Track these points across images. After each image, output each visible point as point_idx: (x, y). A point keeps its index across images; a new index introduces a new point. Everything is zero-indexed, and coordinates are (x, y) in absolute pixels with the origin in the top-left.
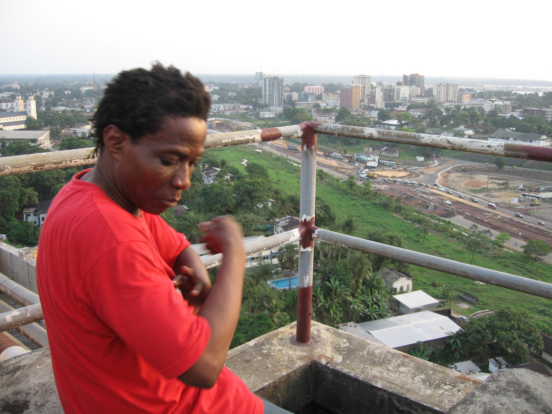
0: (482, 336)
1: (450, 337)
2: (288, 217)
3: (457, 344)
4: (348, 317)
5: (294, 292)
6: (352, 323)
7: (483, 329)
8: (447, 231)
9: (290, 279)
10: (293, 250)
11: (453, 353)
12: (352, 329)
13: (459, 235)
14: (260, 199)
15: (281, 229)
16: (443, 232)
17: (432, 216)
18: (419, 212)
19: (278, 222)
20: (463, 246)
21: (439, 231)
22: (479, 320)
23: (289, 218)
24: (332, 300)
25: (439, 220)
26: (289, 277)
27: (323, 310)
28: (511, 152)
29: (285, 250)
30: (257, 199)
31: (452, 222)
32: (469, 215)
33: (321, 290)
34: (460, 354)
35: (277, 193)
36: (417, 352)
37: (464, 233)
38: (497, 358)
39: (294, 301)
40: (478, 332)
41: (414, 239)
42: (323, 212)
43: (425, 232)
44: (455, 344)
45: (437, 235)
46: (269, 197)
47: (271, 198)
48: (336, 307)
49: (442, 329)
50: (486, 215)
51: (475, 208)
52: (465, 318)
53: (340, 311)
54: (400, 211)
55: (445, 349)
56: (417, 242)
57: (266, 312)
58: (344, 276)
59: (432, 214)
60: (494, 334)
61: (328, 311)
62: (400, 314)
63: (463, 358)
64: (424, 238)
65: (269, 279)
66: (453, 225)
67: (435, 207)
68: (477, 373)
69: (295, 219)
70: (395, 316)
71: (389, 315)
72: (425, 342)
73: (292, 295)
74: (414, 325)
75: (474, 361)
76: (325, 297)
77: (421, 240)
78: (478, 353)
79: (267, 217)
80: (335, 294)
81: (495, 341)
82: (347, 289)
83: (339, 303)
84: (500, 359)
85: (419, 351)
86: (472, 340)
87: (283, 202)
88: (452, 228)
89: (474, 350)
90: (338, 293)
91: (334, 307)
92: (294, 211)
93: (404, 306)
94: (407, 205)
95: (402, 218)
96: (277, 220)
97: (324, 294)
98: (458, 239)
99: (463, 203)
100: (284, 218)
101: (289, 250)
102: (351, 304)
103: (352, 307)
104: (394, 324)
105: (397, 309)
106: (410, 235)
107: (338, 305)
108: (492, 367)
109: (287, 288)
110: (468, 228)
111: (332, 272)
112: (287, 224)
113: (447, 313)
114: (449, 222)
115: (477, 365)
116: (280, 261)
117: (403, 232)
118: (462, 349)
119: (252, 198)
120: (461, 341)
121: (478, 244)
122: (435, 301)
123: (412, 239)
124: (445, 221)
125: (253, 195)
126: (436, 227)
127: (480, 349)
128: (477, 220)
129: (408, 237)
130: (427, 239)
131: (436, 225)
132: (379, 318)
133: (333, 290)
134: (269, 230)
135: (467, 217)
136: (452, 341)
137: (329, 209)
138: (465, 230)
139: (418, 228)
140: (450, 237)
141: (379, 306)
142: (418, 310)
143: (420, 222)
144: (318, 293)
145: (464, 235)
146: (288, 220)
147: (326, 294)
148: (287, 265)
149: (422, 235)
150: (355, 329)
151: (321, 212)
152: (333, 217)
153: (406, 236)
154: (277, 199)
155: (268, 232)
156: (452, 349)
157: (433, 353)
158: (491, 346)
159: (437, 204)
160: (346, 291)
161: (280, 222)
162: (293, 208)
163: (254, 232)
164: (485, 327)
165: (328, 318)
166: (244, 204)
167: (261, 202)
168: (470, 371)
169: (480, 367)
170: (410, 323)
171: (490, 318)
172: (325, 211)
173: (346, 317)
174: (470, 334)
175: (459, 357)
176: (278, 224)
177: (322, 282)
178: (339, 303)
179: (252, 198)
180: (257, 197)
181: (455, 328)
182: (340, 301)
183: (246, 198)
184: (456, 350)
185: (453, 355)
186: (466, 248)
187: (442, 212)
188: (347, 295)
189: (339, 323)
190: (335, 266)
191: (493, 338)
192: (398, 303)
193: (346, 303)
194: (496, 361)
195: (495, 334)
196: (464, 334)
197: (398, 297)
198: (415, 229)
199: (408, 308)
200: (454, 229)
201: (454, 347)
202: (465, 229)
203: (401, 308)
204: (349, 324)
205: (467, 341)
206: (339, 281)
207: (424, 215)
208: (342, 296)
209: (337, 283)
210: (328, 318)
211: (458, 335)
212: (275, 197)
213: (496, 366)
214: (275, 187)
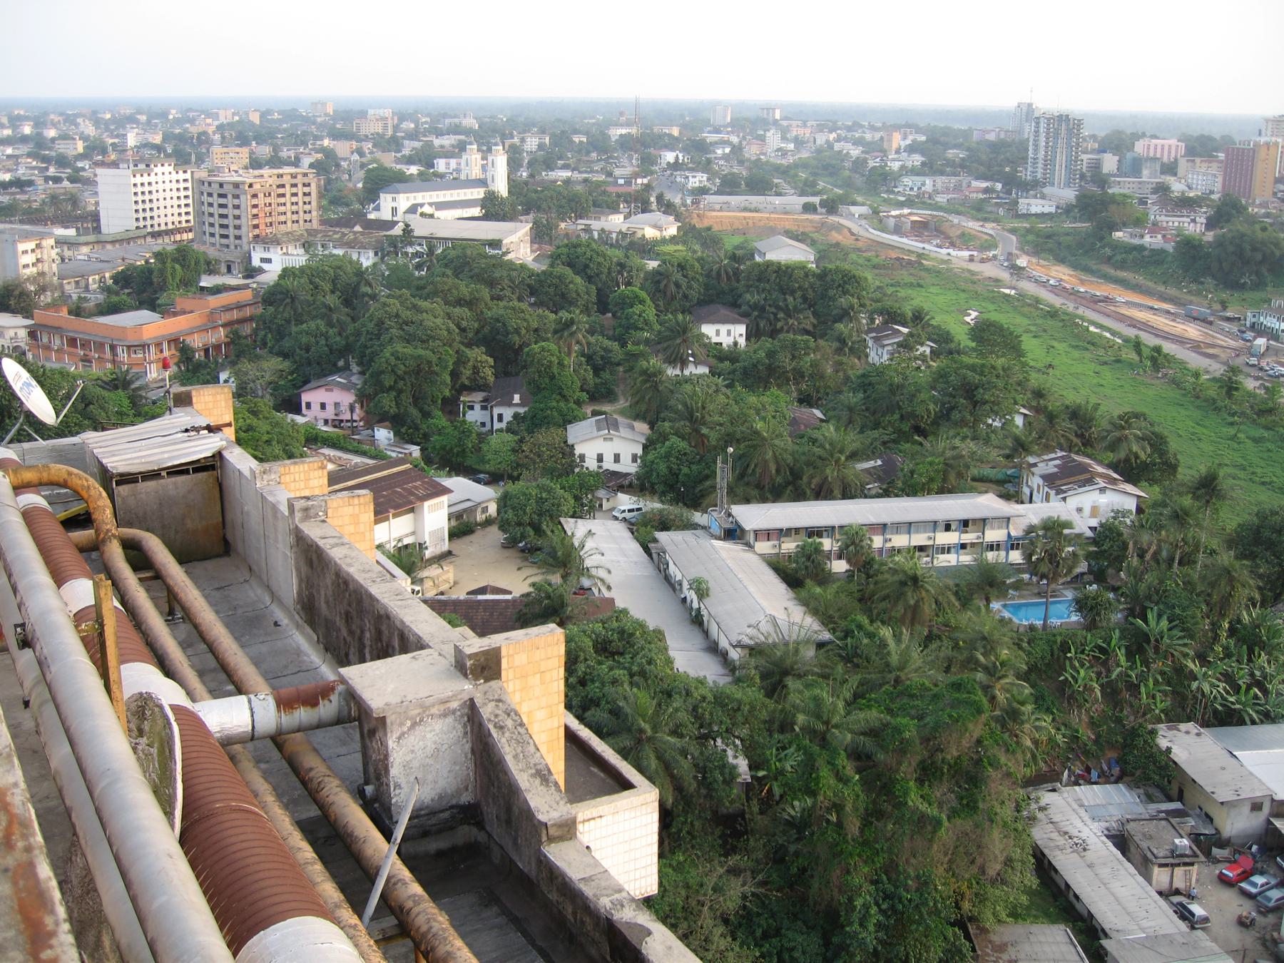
2: (1060, 454)
4: (1183, 709)
5: (1054, 635)
6: (1191, 726)
9: (1046, 603)
10: (1060, 534)
12: (1191, 739)
14: (996, 408)
15: (1041, 482)
19: (1035, 465)
24: (1146, 663)
29: (1040, 533)
30: (987, 407)
33: (1120, 639)
35: (1039, 394)
39: (1052, 655)
42: (1149, 450)
46: (1016, 403)
47: (1024, 407)
48: (1156, 682)
53: (1165, 693)
57: (980, 676)
58: (1184, 610)
61: (1134, 688)
65: (998, 598)
69: (1074, 461)
73: (1048, 641)
76: (1130, 655)
79: (1007, 451)
82: (1186, 641)
83: (1162, 673)
87: (1051, 417)
92: (1078, 441)
96: (1031, 460)
97: (1127, 647)
101: (1049, 534)
102: (1195, 679)
103: (1195, 685)
109: (1039, 623)
111: (1155, 598)
112: (1056, 470)
116: (1028, 557)
119: (975, 404)
125: (978, 397)
133: (1152, 639)
134: (1010, 482)
137: (1166, 442)
144: (1113, 642)
146: (1058, 462)
147: (1134, 648)
148: (1044, 568)
150: (1198, 739)
151: (1144, 449)
152: (1173, 461)
154: (1037, 410)
155: (1010, 488)
160: (1185, 645)
162: (1077, 435)
163: (975, 484)
165: (1132, 706)
166: (956, 415)
167: (996, 414)
173: (1179, 710)
176: (1033, 469)
177: (1127, 617)
178: (1162, 673)
179: (975, 404)
180: (985, 402)
183: (962, 401)
188: (1186, 655)
189: (1159, 721)
190: (1161, 582)
193: (1180, 676)
204: (1183, 726)
206: (1170, 621)
209: (1164, 624)
210: (1132, 706)
212: (1034, 403)
214: (1035, 380)
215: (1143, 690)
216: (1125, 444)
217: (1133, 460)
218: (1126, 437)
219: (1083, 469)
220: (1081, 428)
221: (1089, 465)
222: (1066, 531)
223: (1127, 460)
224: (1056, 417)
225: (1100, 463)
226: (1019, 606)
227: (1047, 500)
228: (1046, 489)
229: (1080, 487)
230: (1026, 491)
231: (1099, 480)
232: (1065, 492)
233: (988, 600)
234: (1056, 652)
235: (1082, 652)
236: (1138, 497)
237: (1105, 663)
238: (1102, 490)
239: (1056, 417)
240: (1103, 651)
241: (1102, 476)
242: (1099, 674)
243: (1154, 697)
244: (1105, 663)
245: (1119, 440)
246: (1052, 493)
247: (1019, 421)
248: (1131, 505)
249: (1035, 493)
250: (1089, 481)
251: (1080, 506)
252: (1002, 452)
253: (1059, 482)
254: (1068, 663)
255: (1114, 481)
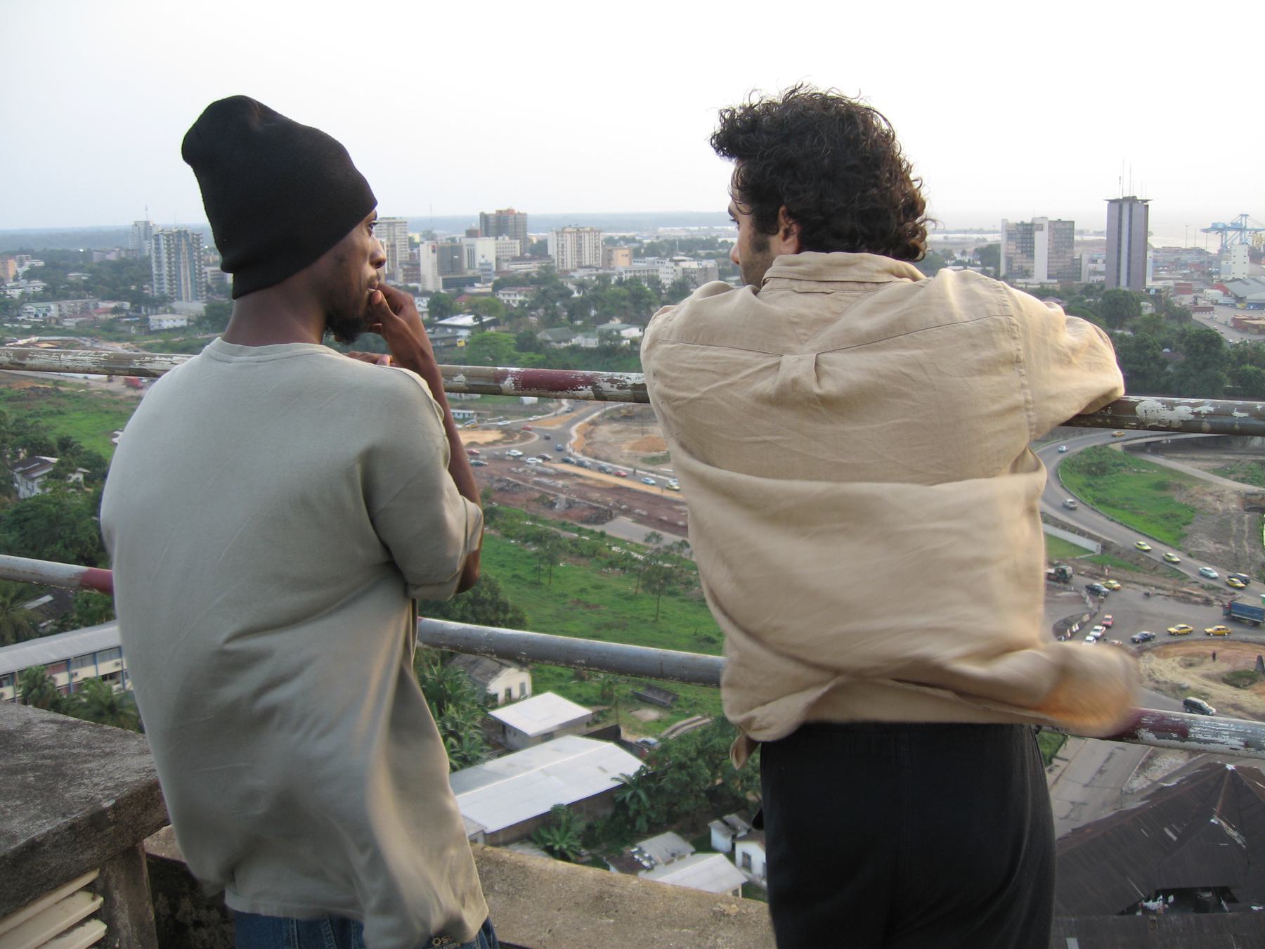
0: (689, 774)
1: (623, 787)
3: (640, 800)
7: (691, 760)
8: (599, 554)
11: (632, 822)
13: (626, 559)
16: (591, 556)
17: (564, 524)
18: (534, 519)
20: (635, 584)
21: (582, 555)
22: (680, 739)
25: (579, 530)
28: (530, 370)
31: (608, 532)
32: (645, 513)
34: (648, 820)
36: (555, 831)
37: (636, 555)
38: (727, 817)
40: (681, 766)
41: (529, 579)
43: (552, 561)
44: (635, 800)
45: (579, 565)
49: (604, 771)
50: (681, 511)
51: (656, 496)
52: (652, 740)
54: (492, 518)
55: (614, 816)
56: (536, 584)
59: (563, 520)
60: (715, 767)
62: (510, 750)
63: (655, 829)
64: (550, 574)
66: (611, 538)
67: (570, 505)
68: (688, 855)
70: (499, 756)
71: (484, 756)
72: (570, 805)
74: (542, 770)
75: (680, 832)
77: (545, 580)
78: (687, 813)
81: (719, 781)
84: (733, 818)
85: (558, 828)
86: (669, 786)
88: (610, 547)
89: (676, 808)
93: (516, 732)
94: (507, 505)
95: (498, 534)
98: (623, 569)
99: (629, 490)
104: (496, 775)
105: (500, 740)
106: (515, 572)
108: (719, 838)
110: (641, 542)
113: (612, 735)
114: (602, 535)
115: (686, 839)
117: (503, 566)
118: (652, 807)
120: (648, 791)
121: (668, 576)
122: (581, 711)
123: (524, 580)
124: (592, 532)
126: (574, 548)
127: (689, 804)
128: (663, 524)
129: (514, 576)
130: (558, 577)
131: (574, 543)
132: (462, 767)
135: (640, 520)
136: (629, 794)
138: (638, 548)
139: (537, 554)
140: (607, 567)
141: (459, 739)
142: (547, 736)
143: (539, 539)
145: (636, 560)
149: (545, 567)
153: (509, 574)
156: (631, 813)
157: (590, 828)
158: (713, 794)
159: (573, 497)
164: (693, 754)
168: (673, 855)
169: (694, 843)
170: (531, 768)
171: (704, 733)
174: (665, 773)
175: (645, 827)
181: (630, 765)
184: (638, 813)
185: (634, 826)
186: (643, 587)
187: (585, 513)
191: (714, 774)
192: (503, 727)
194: (726, 823)
195: (716, 767)
196: (652, 777)
197: (501, 714)
198: (529, 557)
199: (525, 735)
200: (614, 548)
201: (633, 807)
202: (638, 546)
203: (510, 738)
205: (660, 791)
207: (545, 522)
211: (640, 780)
213: (725, 835)
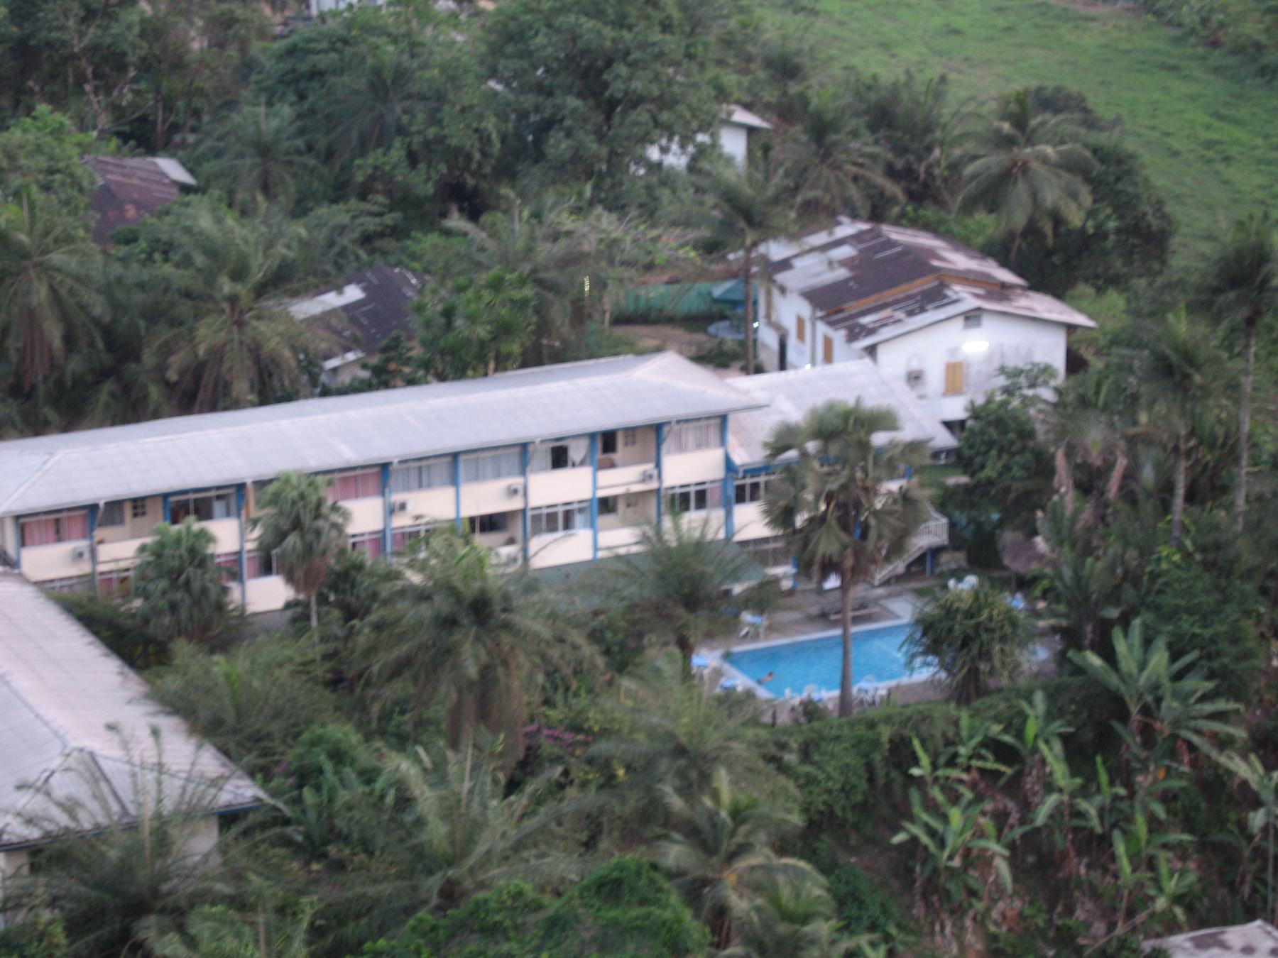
2: (847, 228)
5: (872, 725)
9: (845, 640)
10: (864, 446)
14: (665, 116)
15: (805, 309)
19: (785, 265)
23: (856, 238)
24: (1122, 774)
26: (842, 623)
27: (1061, 841)
29: (812, 446)
30: (641, 115)
33: (1050, 716)
39: (871, 780)
42: (1087, 199)
46: (722, 94)
47: (748, 107)
48: (1155, 825)
53: (1181, 852)
57: (676, 853)
69: (891, 244)
76: (1077, 755)
79: (704, 233)
80: (1147, 734)
83: (1167, 798)
87: (821, 129)
90: (1163, 727)
91: (1141, 826)
92: (894, 189)
96: (776, 250)
100: (820, 238)
101: (834, 449)
107: (1160, 811)
109: (828, 695)
112: (842, 273)
116: (782, 516)
119: (609, 107)
125: (617, 89)
133: (1134, 709)
134: (723, 317)
137: (1129, 172)
144: (1031, 729)
146: (846, 251)
147: (1088, 735)
148: (828, 544)
151: (1074, 196)
152: (1155, 223)
154: (786, 112)
155: (724, 333)
161: (798, 263)
162: (891, 172)
163: (621, 331)
166: (558, 145)
167: (670, 131)
172: (1096, 184)
176: (781, 277)
177: (1061, 658)
179: (609, 107)
180: (636, 102)
182: (1176, 784)
183: (573, 102)
190: (1146, 551)
208: (1192, 747)
209: (1159, 658)
215: (1120, 848)
216: (1020, 191)
217: (1048, 228)
218: (1025, 168)
219: (916, 263)
220: (901, 150)
221: (932, 253)
222: (879, 439)
223: (1031, 230)
224: (833, 126)
225: (962, 243)
226: (773, 655)
227: (828, 358)
228: (822, 328)
229: (911, 313)
230: (768, 338)
231: (957, 290)
232: (871, 331)
233: (686, 647)
234: (881, 772)
235: (952, 762)
236: (1070, 328)
237: (1014, 787)
238: (972, 318)
239: (833, 126)
240: (1004, 753)
241: (966, 278)
242: (1000, 818)
243: (1151, 864)
244: (1014, 787)
245: (1006, 177)
246: (839, 336)
247: (734, 145)
248: (1051, 350)
249: (792, 342)
250: (934, 297)
251: (915, 365)
252: (692, 235)
253: (852, 307)
254: (915, 795)
255: (1000, 291)
